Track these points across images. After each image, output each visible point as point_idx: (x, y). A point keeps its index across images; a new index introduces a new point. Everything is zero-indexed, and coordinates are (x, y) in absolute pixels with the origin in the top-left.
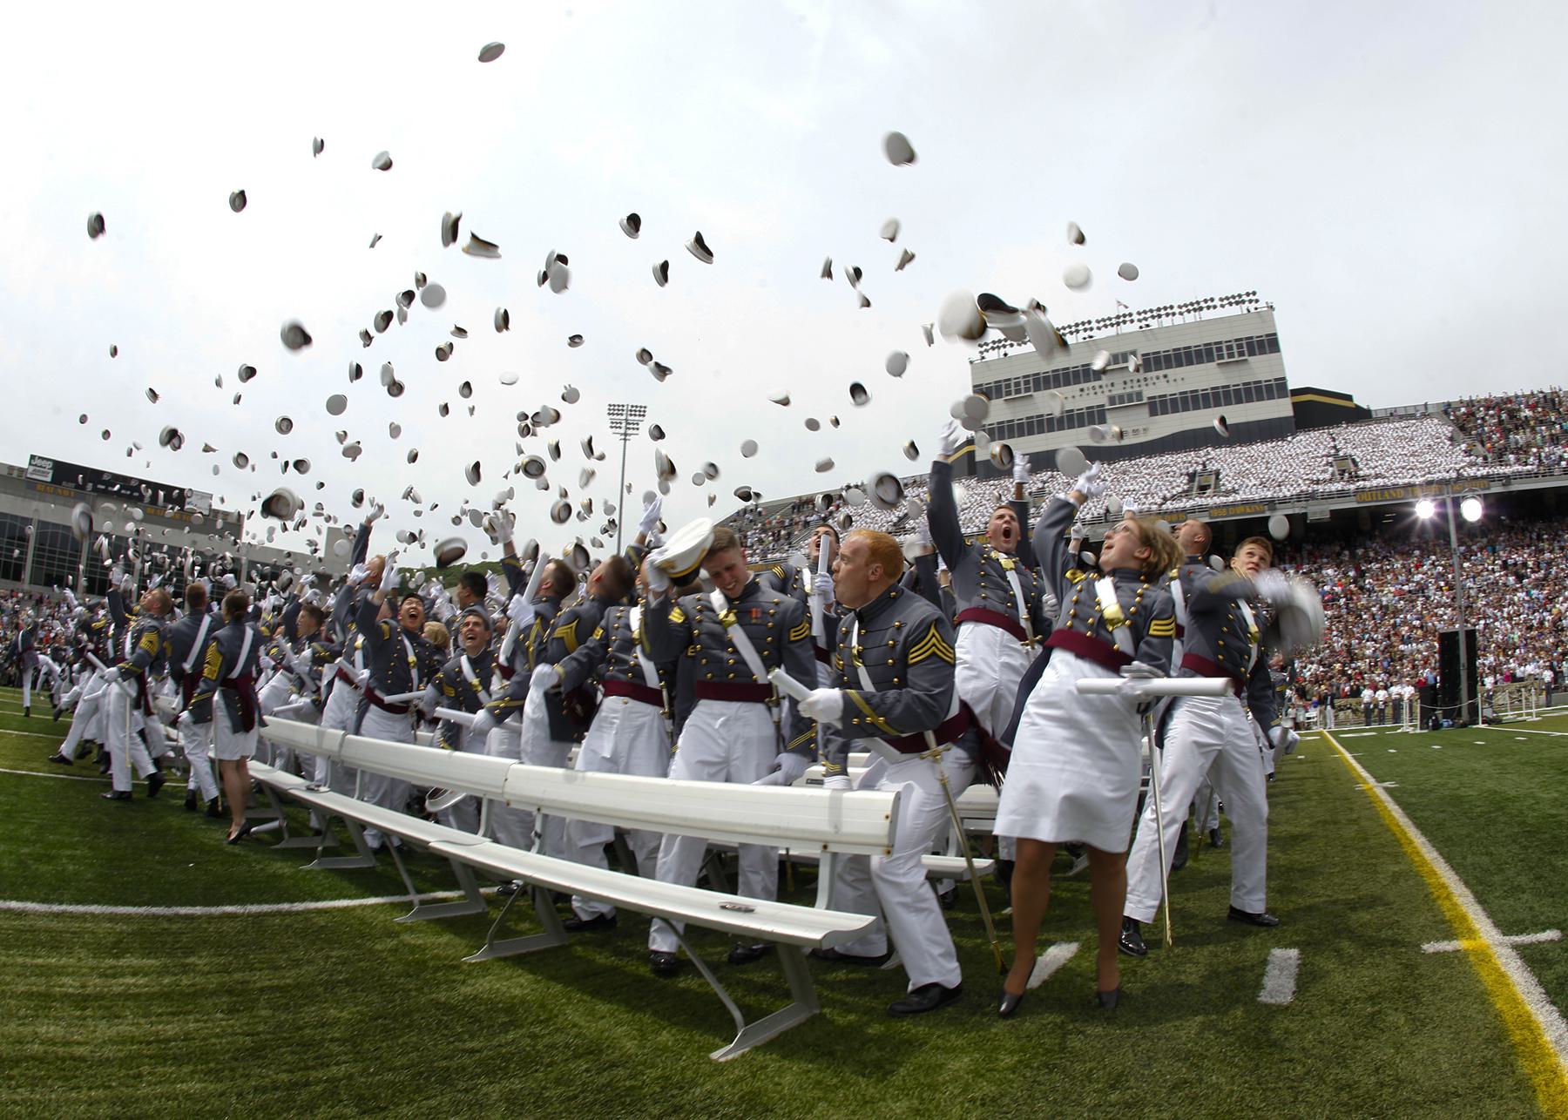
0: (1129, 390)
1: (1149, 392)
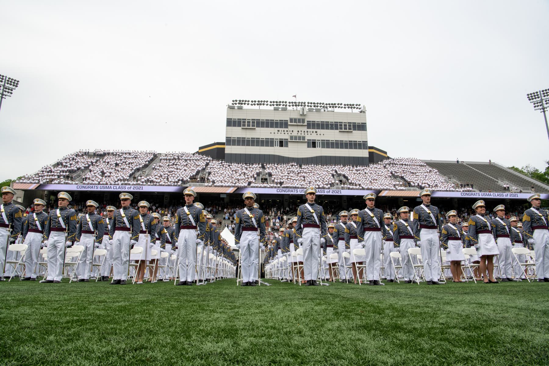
0: (299, 135)
1: (308, 137)
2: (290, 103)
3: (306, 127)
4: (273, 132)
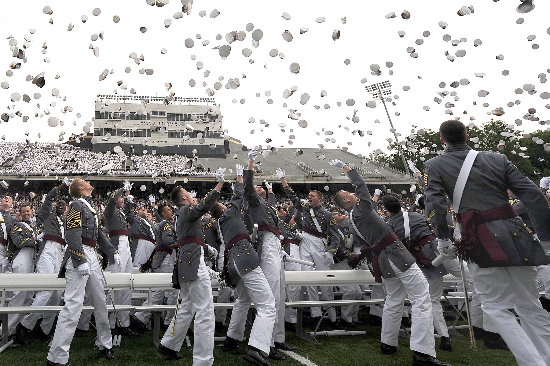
2: (151, 97)
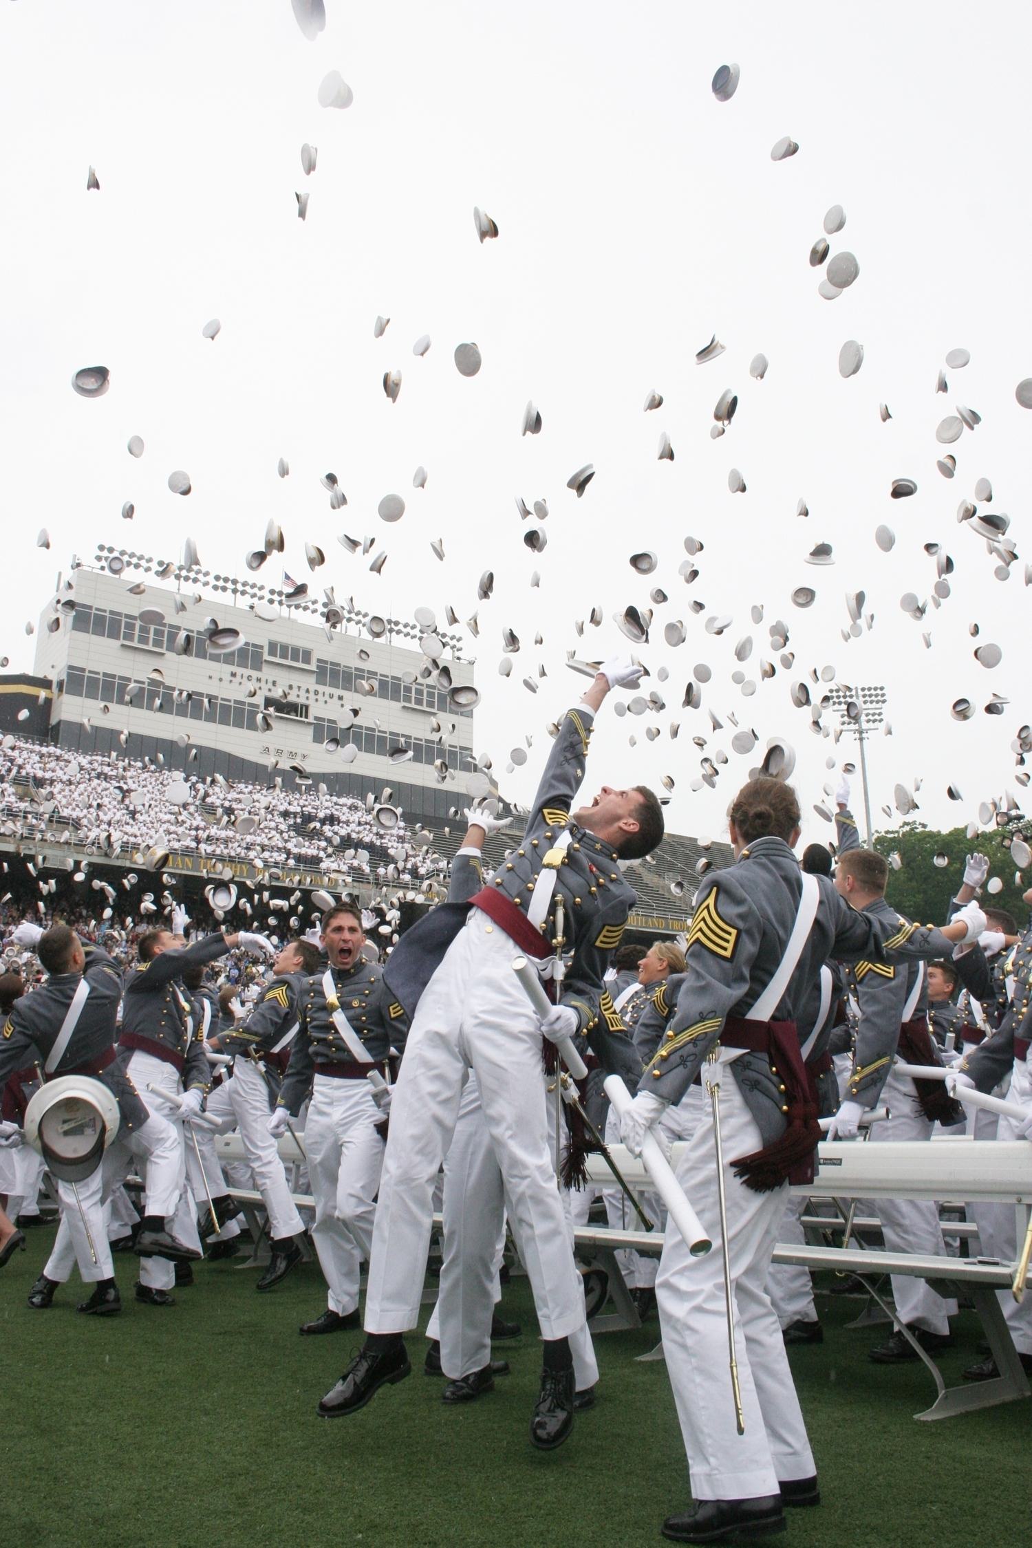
3: (313, 679)
4: (216, 676)
